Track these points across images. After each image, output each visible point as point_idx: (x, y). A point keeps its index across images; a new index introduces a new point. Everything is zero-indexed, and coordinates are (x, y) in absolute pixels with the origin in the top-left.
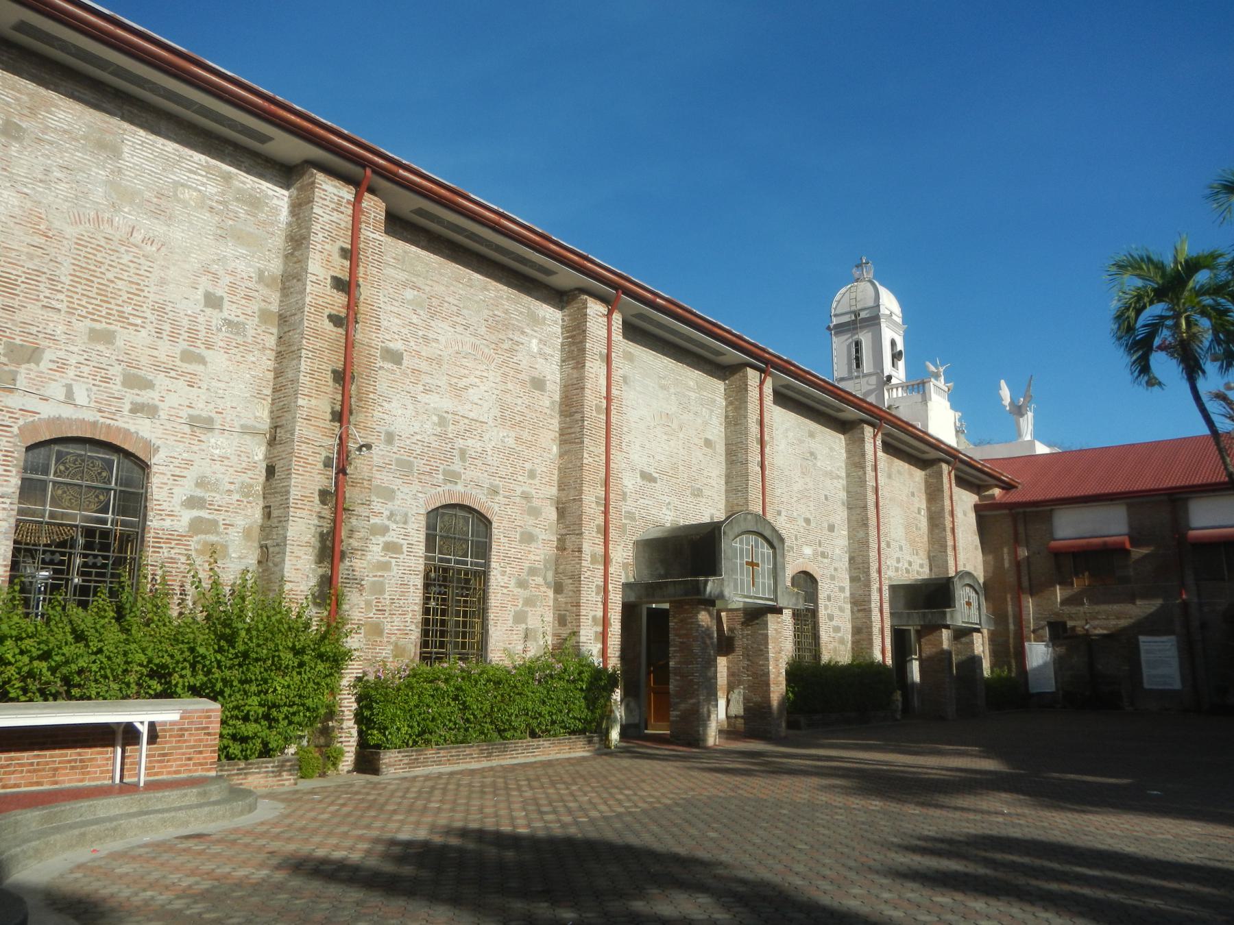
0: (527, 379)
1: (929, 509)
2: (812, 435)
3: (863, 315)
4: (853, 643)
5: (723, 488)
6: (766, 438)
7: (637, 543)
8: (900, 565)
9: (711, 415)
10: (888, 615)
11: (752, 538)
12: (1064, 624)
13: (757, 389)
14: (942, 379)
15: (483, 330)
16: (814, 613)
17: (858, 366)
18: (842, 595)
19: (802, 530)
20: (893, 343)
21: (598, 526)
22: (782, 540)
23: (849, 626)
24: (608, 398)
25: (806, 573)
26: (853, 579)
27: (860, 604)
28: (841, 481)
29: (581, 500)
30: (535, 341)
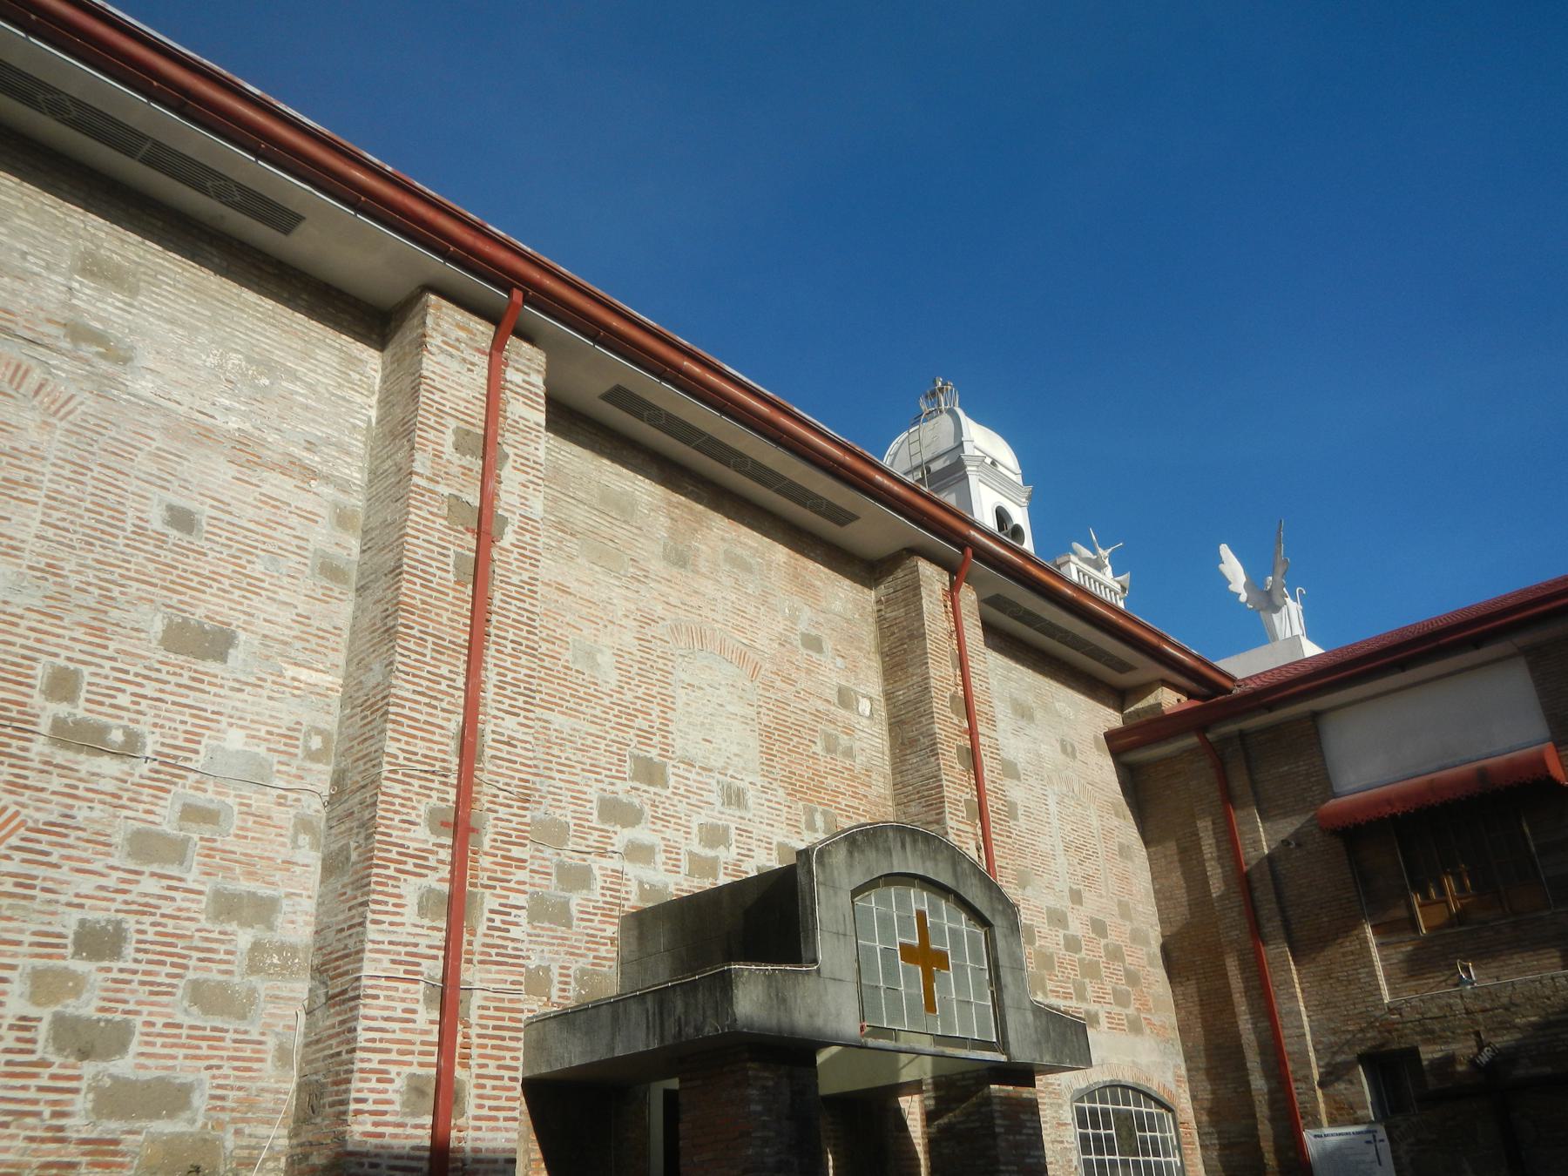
1: (889, 696)
3: (936, 466)
12: (1413, 1053)
14: (1109, 570)
18: (244, 938)
26: (332, 866)
28: (328, 491)
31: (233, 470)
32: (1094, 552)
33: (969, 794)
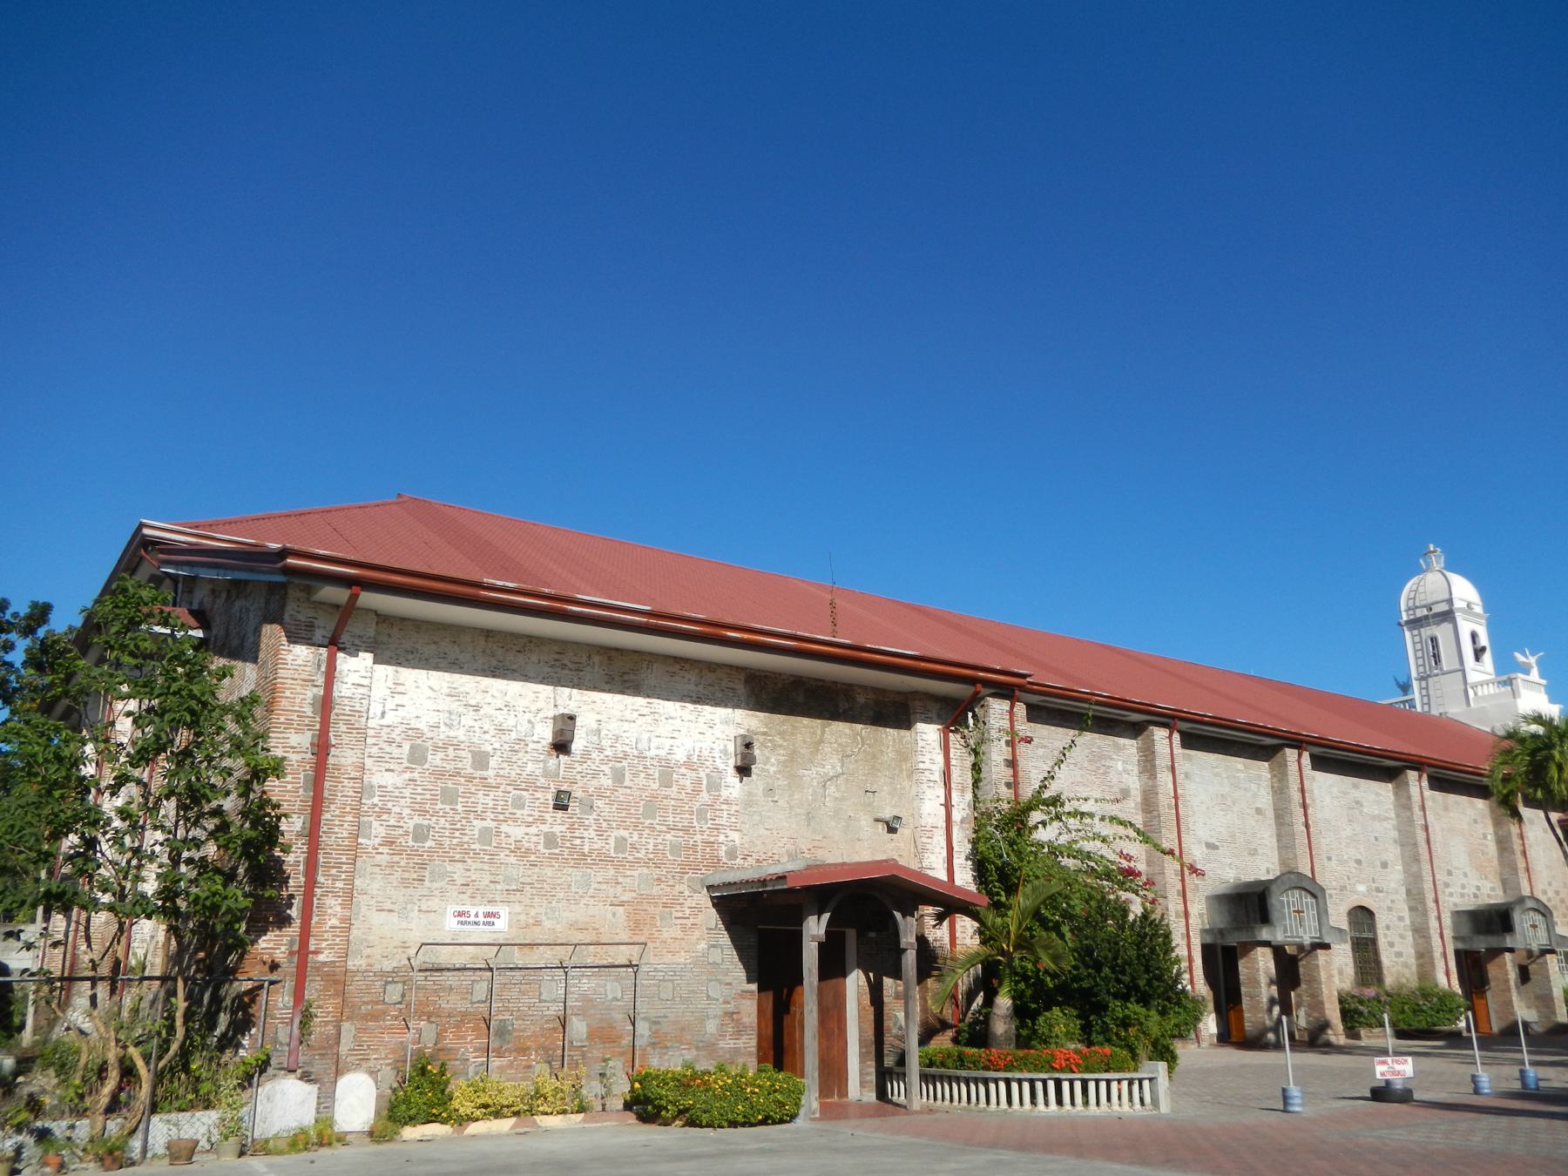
0: (1117, 790)
1: (1496, 833)
2: (1356, 786)
3: (1437, 609)
4: (1417, 966)
5: (1276, 845)
6: (1308, 801)
7: (1207, 898)
8: (1466, 891)
9: (1259, 789)
10: (1451, 940)
11: (1297, 893)
13: (1296, 763)
15: (1086, 764)
16: (1374, 941)
17: (1436, 663)
18: (1402, 924)
19: (1354, 871)
20: (1474, 636)
21: (1178, 891)
22: (1323, 890)
23: (1412, 951)
24: (1176, 797)
25: (1362, 908)
26: (1411, 909)
27: (1420, 931)
28: (1390, 822)
29: (1164, 873)
30: (1120, 763)
31: (1378, 824)
32: (1526, 657)
33: (1524, 865)
